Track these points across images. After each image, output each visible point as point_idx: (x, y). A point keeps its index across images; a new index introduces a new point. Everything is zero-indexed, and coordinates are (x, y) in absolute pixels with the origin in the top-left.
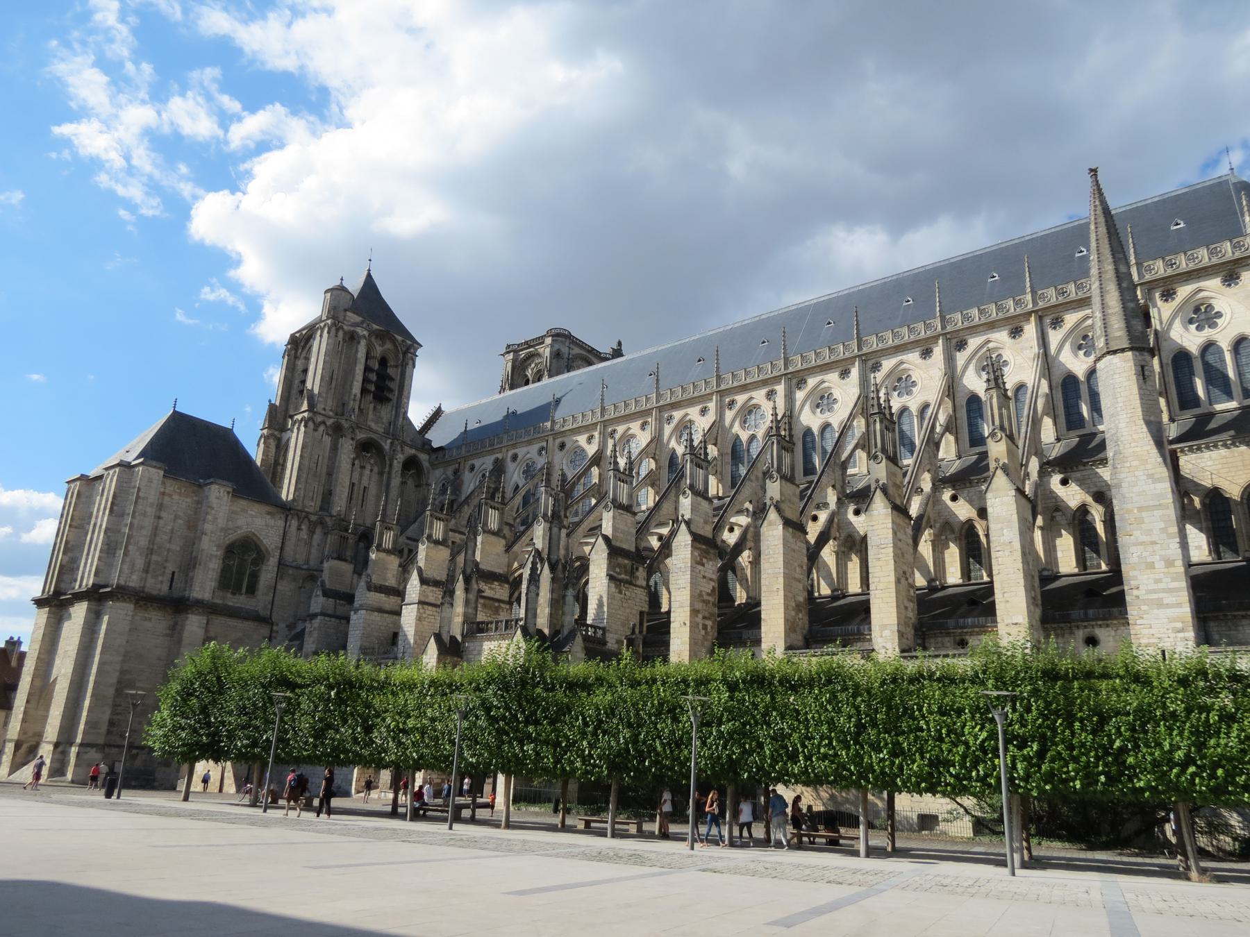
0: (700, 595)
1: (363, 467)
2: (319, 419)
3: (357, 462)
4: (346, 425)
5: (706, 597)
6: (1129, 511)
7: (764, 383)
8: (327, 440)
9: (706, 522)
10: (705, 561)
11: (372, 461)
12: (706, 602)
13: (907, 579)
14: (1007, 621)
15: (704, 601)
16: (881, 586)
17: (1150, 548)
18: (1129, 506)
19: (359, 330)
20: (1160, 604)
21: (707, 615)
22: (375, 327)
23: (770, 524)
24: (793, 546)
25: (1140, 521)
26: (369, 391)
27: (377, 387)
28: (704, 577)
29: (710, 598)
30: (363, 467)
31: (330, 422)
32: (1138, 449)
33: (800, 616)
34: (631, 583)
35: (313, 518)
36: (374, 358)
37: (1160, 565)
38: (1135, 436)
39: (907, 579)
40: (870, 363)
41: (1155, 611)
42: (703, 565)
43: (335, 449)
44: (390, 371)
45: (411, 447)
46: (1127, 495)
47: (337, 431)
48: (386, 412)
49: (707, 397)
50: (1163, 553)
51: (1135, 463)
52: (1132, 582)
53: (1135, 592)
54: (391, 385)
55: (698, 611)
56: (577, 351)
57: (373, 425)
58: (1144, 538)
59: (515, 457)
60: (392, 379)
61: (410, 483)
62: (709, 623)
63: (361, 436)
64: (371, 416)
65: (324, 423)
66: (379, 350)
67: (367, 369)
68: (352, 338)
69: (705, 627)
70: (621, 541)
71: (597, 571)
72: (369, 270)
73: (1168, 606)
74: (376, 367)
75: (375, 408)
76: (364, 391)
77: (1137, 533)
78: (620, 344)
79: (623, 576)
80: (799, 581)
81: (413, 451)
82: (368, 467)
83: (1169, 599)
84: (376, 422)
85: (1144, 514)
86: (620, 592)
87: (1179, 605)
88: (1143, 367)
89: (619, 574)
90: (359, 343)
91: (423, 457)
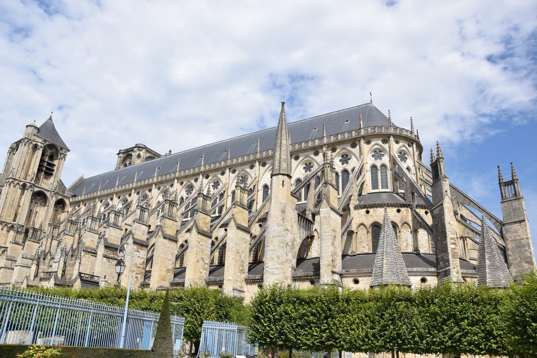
0: (136, 264)
2: (16, 182)
3: (33, 201)
4: (28, 185)
5: (138, 265)
6: (270, 238)
8: (19, 191)
9: (143, 234)
10: (140, 250)
11: (41, 201)
12: (139, 267)
13: (204, 261)
14: (227, 279)
15: (137, 267)
16: (190, 263)
17: (273, 252)
18: (270, 235)
19: (39, 144)
20: (273, 274)
21: (138, 272)
23: (159, 237)
24: (168, 246)
25: (272, 242)
27: (47, 168)
28: (139, 257)
29: (141, 266)
31: (21, 183)
32: (276, 213)
33: (169, 274)
36: (47, 155)
37: (275, 258)
38: (276, 208)
39: (204, 261)
40: (232, 170)
41: (272, 276)
42: (139, 252)
45: (61, 195)
46: (270, 231)
47: (24, 187)
49: (173, 180)
50: (277, 254)
51: (274, 219)
52: (267, 265)
53: (267, 269)
55: (133, 271)
56: (148, 155)
58: (273, 248)
60: (55, 165)
62: (139, 276)
63: (36, 189)
65: (18, 184)
66: (49, 152)
67: (42, 161)
68: (35, 147)
69: (137, 278)
70: (113, 241)
71: (100, 253)
72: (51, 117)
73: (276, 274)
76: (40, 170)
77: (270, 246)
79: (112, 255)
80: (170, 260)
83: (276, 272)
85: (274, 239)
86: (109, 262)
87: (278, 274)
88: (283, 181)
89: (110, 254)
90: (39, 149)
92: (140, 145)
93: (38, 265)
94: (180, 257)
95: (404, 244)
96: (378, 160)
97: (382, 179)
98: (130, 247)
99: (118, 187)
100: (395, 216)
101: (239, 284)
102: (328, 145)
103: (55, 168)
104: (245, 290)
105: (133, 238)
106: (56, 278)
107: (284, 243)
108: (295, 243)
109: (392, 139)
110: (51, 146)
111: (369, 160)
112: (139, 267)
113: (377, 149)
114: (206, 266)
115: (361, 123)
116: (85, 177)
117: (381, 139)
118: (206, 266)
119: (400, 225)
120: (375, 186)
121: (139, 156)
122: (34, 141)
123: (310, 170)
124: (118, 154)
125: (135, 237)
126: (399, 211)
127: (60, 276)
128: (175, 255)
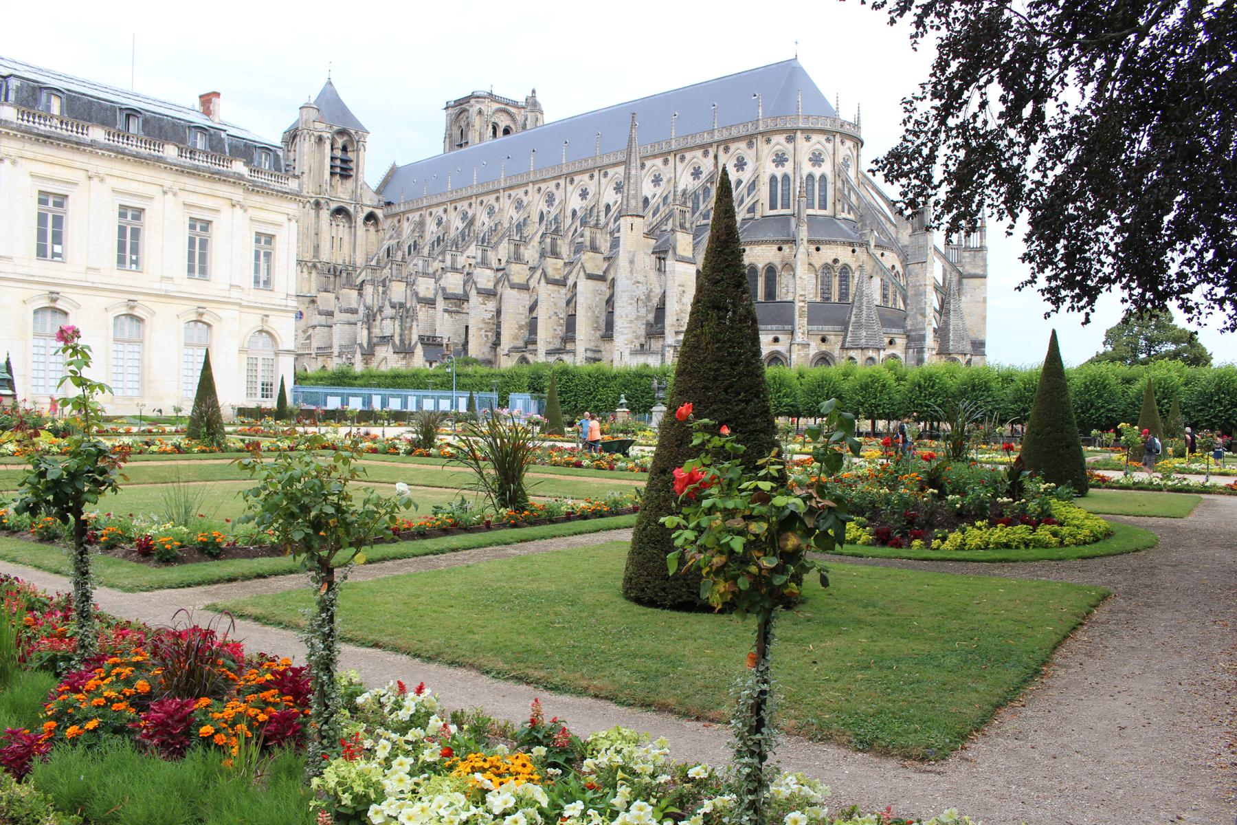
0: (483, 320)
1: (337, 225)
4: (322, 201)
7: (554, 178)
8: (313, 212)
9: (488, 281)
20: (623, 334)
22: (335, 128)
26: (336, 173)
27: (342, 169)
30: (337, 225)
31: (312, 201)
34: (459, 312)
35: (310, 264)
43: (318, 216)
44: (351, 155)
48: (349, 184)
54: (352, 165)
56: (496, 106)
57: (342, 196)
59: (431, 214)
60: (351, 161)
61: (372, 229)
62: (490, 334)
63: (334, 206)
64: (340, 189)
66: (340, 142)
67: (333, 159)
69: (487, 336)
74: (339, 153)
75: (342, 183)
76: (332, 174)
78: (534, 91)
81: (370, 209)
82: (342, 224)
84: (343, 193)
91: (379, 213)
92: (478, 94)
93: (369, 329)
94: (532, 308)
95: (784, 291)
96: (780, 167)
97: (782, 195)
98: (474, 298)
99: (451, 192)
100: (775, 255)
101: (593, 344)
102: (719, 143)
103: (352, 165)
104: (602, 349)
105: (477, 288)
106: (394, 345)
107: (632, 299)
108: (652, 294)
109: (799, 134)
110: (342, 133)
111: (769, 169)
112: (488, 323)
113: (780, 150)
114: (562, 321)
115: (760, 111)
116: (400, 164)
117: (785, 135)
118: (562, 321)
119: (780, 267)
120: (773, 207)
121: (480, 112)
122: (315, 130)
123: (699, 178)
124: (446, 108)
125: (479, 286)
126: (780, 249)
127: (397, 342)
128: (527, 307)
